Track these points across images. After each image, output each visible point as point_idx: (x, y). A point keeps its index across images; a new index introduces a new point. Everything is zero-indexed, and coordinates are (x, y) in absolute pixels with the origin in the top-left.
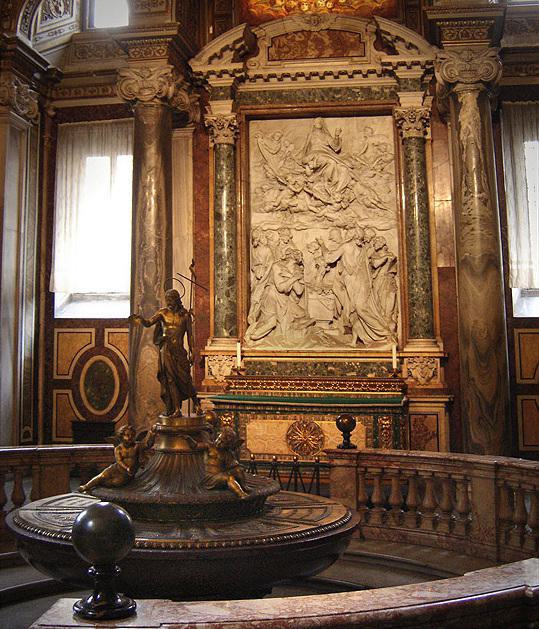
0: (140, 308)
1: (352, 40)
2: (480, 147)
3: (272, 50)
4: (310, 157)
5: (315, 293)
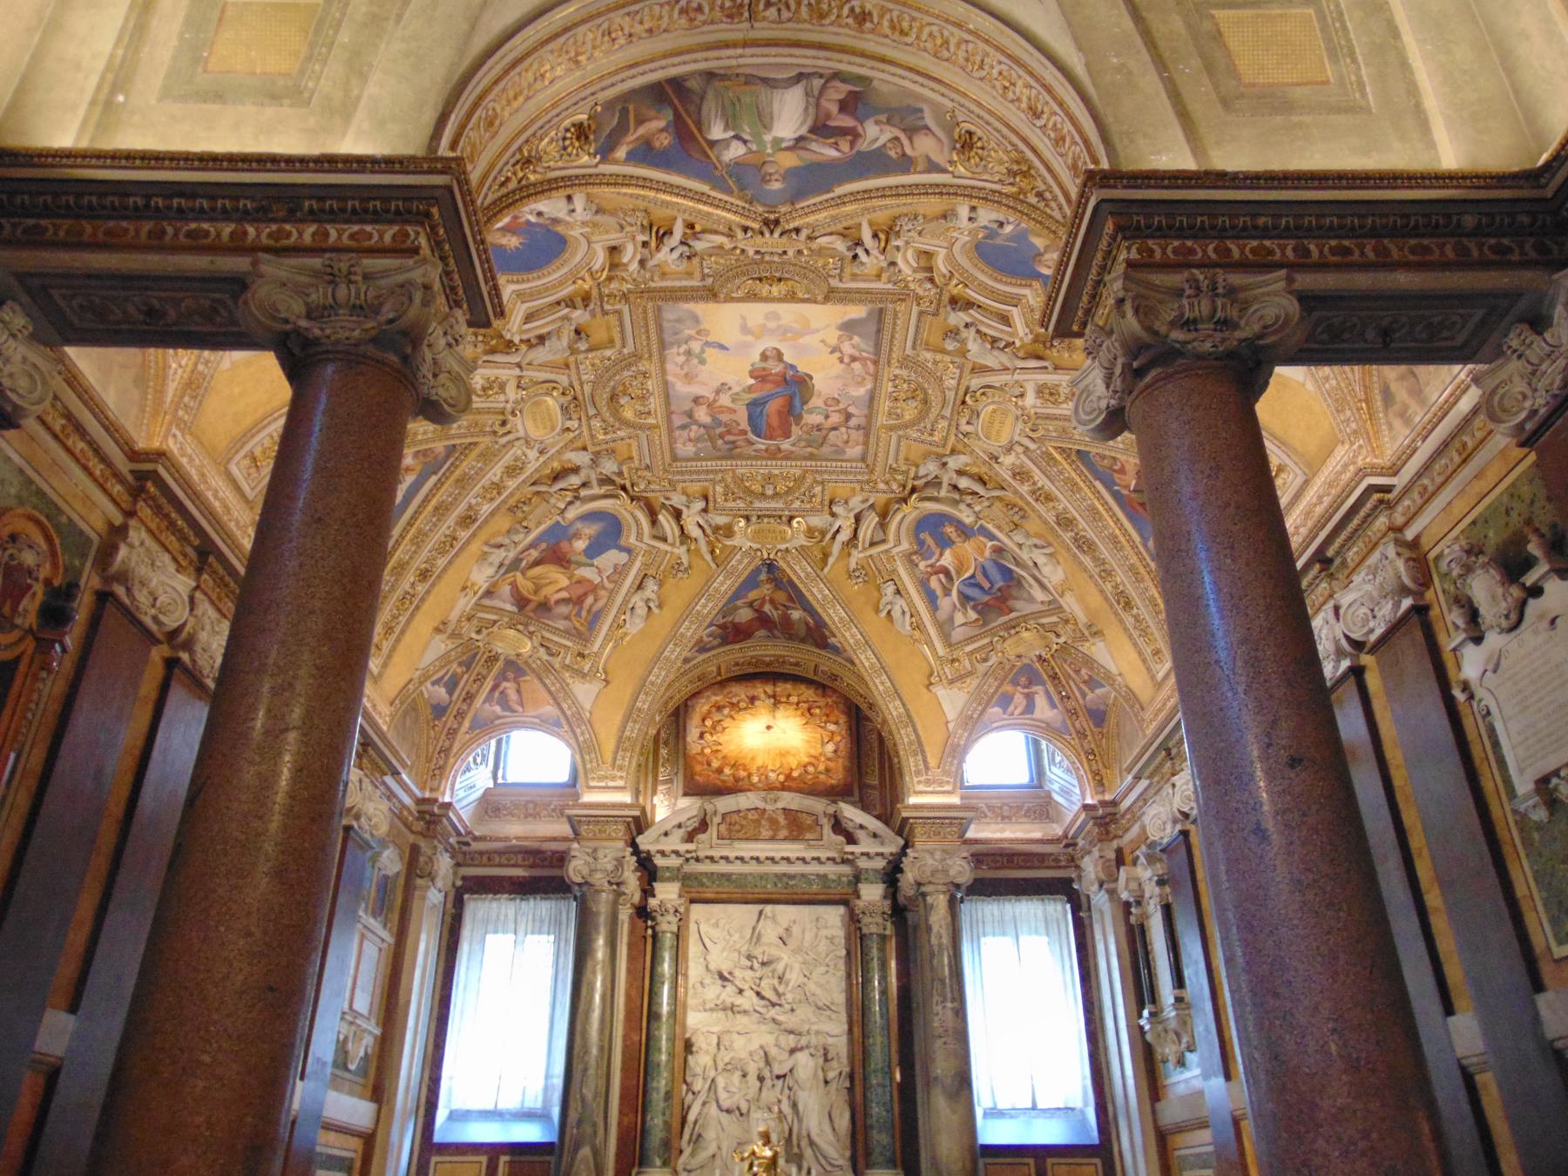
0: (575, 1131)
1: (809, 822)
3: (723, 828)
5: (760, 1112)
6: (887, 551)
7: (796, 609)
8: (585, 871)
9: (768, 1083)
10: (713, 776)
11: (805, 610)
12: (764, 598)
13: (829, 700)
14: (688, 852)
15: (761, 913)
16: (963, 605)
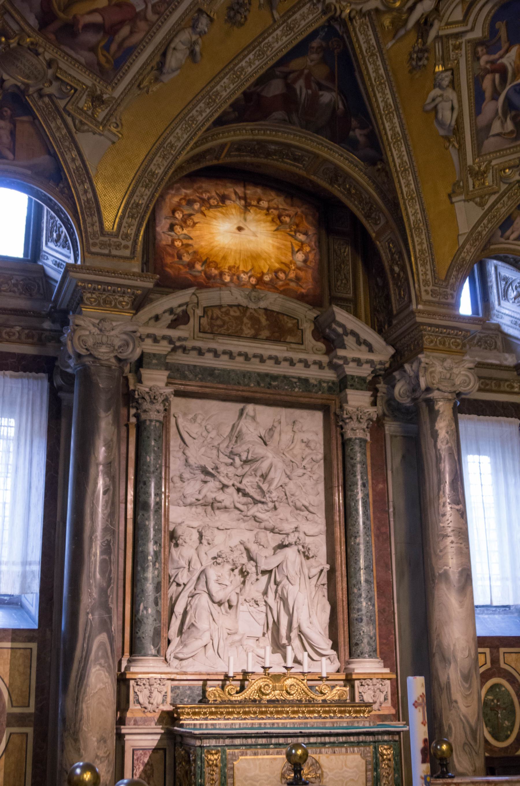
1: (290, 325)
2: (456, 458)
3: (204, 321)
4: (245, 447)
6: (457, 36)
7: (328, 89)
8: (90, 342)
9: (252, 577)
10: (184, 270)
11: (341, 92)
12: (302, 71)
13: (299, 211)
14: (180, 339)
15: (242, 412)
16: (505, 115)
